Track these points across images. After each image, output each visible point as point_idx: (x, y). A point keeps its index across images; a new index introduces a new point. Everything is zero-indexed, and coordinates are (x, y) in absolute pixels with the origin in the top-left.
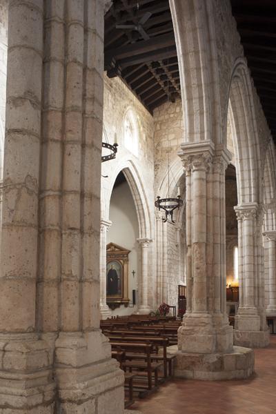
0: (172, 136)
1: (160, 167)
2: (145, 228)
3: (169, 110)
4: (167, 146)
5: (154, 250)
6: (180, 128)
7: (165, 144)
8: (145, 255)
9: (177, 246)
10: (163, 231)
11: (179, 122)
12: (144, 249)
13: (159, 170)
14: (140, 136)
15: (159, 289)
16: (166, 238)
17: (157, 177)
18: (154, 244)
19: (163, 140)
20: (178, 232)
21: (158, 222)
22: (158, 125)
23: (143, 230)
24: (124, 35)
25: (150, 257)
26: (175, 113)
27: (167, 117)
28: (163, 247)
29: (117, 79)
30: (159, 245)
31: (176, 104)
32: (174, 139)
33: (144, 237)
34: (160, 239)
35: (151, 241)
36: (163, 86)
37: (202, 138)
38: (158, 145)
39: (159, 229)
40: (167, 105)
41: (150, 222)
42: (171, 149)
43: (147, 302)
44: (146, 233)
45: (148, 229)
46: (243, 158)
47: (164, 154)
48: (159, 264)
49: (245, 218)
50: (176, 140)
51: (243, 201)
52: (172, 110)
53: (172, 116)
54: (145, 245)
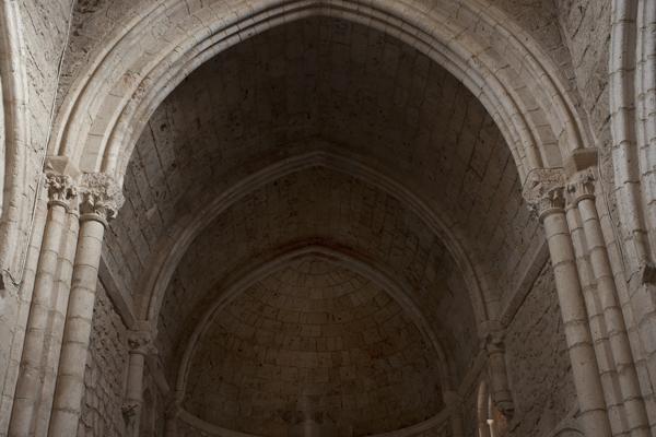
9: (127, 414)
10: (76, 267)
16: (87, 301)
20: (139, 360)
21: (59, 213)
30: (41, 320)
39: (54, 243)
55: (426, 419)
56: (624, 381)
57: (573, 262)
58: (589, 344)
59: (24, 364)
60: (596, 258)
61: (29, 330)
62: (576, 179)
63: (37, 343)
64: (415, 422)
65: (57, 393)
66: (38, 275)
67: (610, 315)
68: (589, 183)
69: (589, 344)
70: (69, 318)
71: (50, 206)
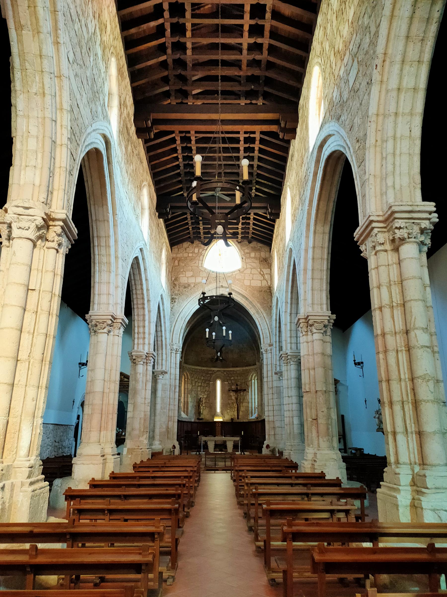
0: (189, 274)
1: (176, 300)
2: (162, 360)
3: (188, 249)
4: (186, 282)
5: (168, 382)
6: (198, 267)
7: (183, 280)
8: (160, 387)
10: (176, 364)
11: (197, 262)
12: (159, 381)
13: (175, 304)
14: (166, 270)
15: (170, 423)
17: (173, 310)
18: (167, 376)
19: (181, 275)
22: (176, 262)
23: (160, 361)
24: (182, 187)
25: (164, 390)
26: (193, 252)
27: (186, 255)
28: (175, 379)
29: (161, 220)
30: (172, 377)
31: (195, 245)
32: (192, 276)
33: (160, 369)
34: (173, 371)
35: (166, 373)
36: (191, 229)
37: (322, 308)
38: (176, 279)
39: (172, 361)
40: (186, 244)
41: (166, 354)
42: (189, 285)
43: (158, 437)
44: (162, 365)
45: (164, 362)
46: (293, 312)
47: (181, 289)
48: (171, 397)
49: (292, 363)
50: (194, 278)
51: (291, 348)
52: (190, 250)
53: (190, 255)
54: (161, 377)
55: (253, 365)
56: (271, 390)
57: (267, 365)
58: (267, 382)
59: (170, 385)
60: (270, 365)
61: (170, 379)
62: (269, 348)
63: (172, 381)
64: (250, 365)
65: (175, 389)
66: (171, 367)
67: (271, 377)
68: (271, 350)
69: (267, 382)
70: (175, 374)
71: (171, 353)
